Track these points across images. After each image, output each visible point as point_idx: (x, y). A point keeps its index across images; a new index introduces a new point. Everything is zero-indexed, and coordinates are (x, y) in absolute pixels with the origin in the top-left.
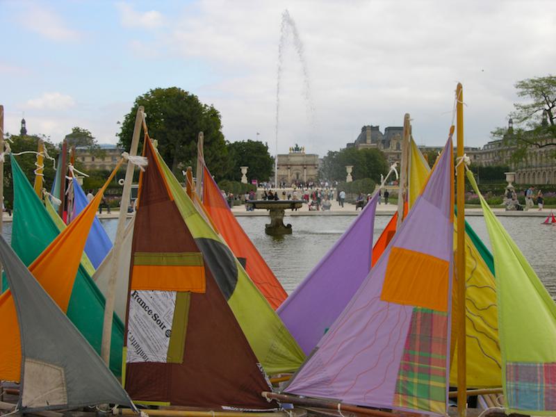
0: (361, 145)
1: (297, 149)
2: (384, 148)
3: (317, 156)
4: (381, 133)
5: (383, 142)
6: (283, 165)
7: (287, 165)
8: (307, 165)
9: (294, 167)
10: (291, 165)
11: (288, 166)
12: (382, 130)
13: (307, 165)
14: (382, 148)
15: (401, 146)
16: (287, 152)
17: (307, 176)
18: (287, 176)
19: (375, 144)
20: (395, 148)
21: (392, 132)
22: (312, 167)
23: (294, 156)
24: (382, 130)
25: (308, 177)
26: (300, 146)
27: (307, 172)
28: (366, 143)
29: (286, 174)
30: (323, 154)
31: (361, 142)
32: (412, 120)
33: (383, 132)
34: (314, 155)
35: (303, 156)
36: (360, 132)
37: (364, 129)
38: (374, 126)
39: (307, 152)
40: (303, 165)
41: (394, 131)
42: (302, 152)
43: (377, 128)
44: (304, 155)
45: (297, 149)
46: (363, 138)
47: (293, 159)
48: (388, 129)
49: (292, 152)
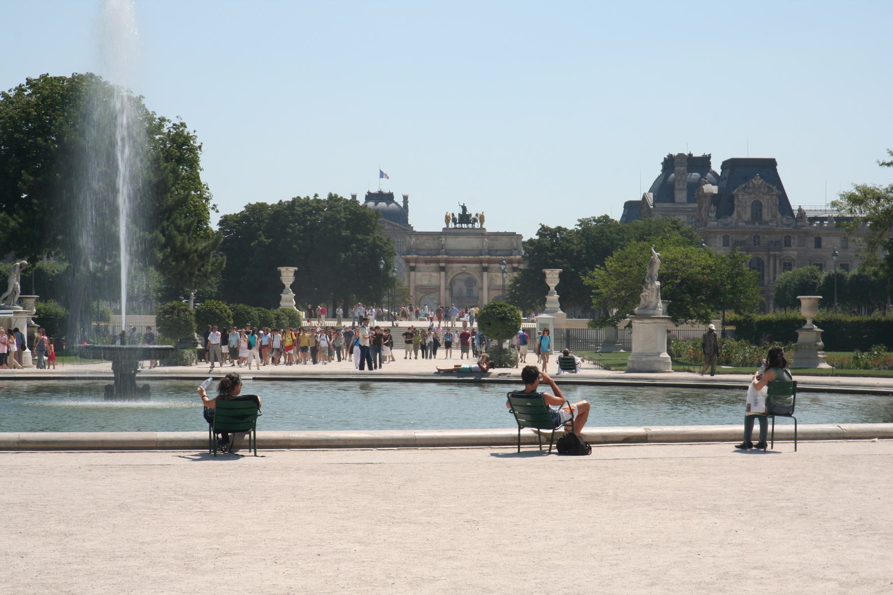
1: (465, 217)
2: (718, 217)
3: (520, 236)
4: (715, 174)
12: (716, 167)
13: (489, 262)
14: (713, 215)
15: (765, 211)
16: (438, 226)
19: (696, 205)
20: (747, 216)
24: (716, 167)
26: (472, 211)
28: (672, 200)
29: (434, 282)
30: (530, 233)
33: (719, 172)
37: (670, 163)
38: (697, 154)
39: (490, 226)
42: (477, 225)
44: (481, 233)
45: (465, 217)
46: (663, 189)
47: (453, 243)
48: (731, 165)
49: (451, 225)
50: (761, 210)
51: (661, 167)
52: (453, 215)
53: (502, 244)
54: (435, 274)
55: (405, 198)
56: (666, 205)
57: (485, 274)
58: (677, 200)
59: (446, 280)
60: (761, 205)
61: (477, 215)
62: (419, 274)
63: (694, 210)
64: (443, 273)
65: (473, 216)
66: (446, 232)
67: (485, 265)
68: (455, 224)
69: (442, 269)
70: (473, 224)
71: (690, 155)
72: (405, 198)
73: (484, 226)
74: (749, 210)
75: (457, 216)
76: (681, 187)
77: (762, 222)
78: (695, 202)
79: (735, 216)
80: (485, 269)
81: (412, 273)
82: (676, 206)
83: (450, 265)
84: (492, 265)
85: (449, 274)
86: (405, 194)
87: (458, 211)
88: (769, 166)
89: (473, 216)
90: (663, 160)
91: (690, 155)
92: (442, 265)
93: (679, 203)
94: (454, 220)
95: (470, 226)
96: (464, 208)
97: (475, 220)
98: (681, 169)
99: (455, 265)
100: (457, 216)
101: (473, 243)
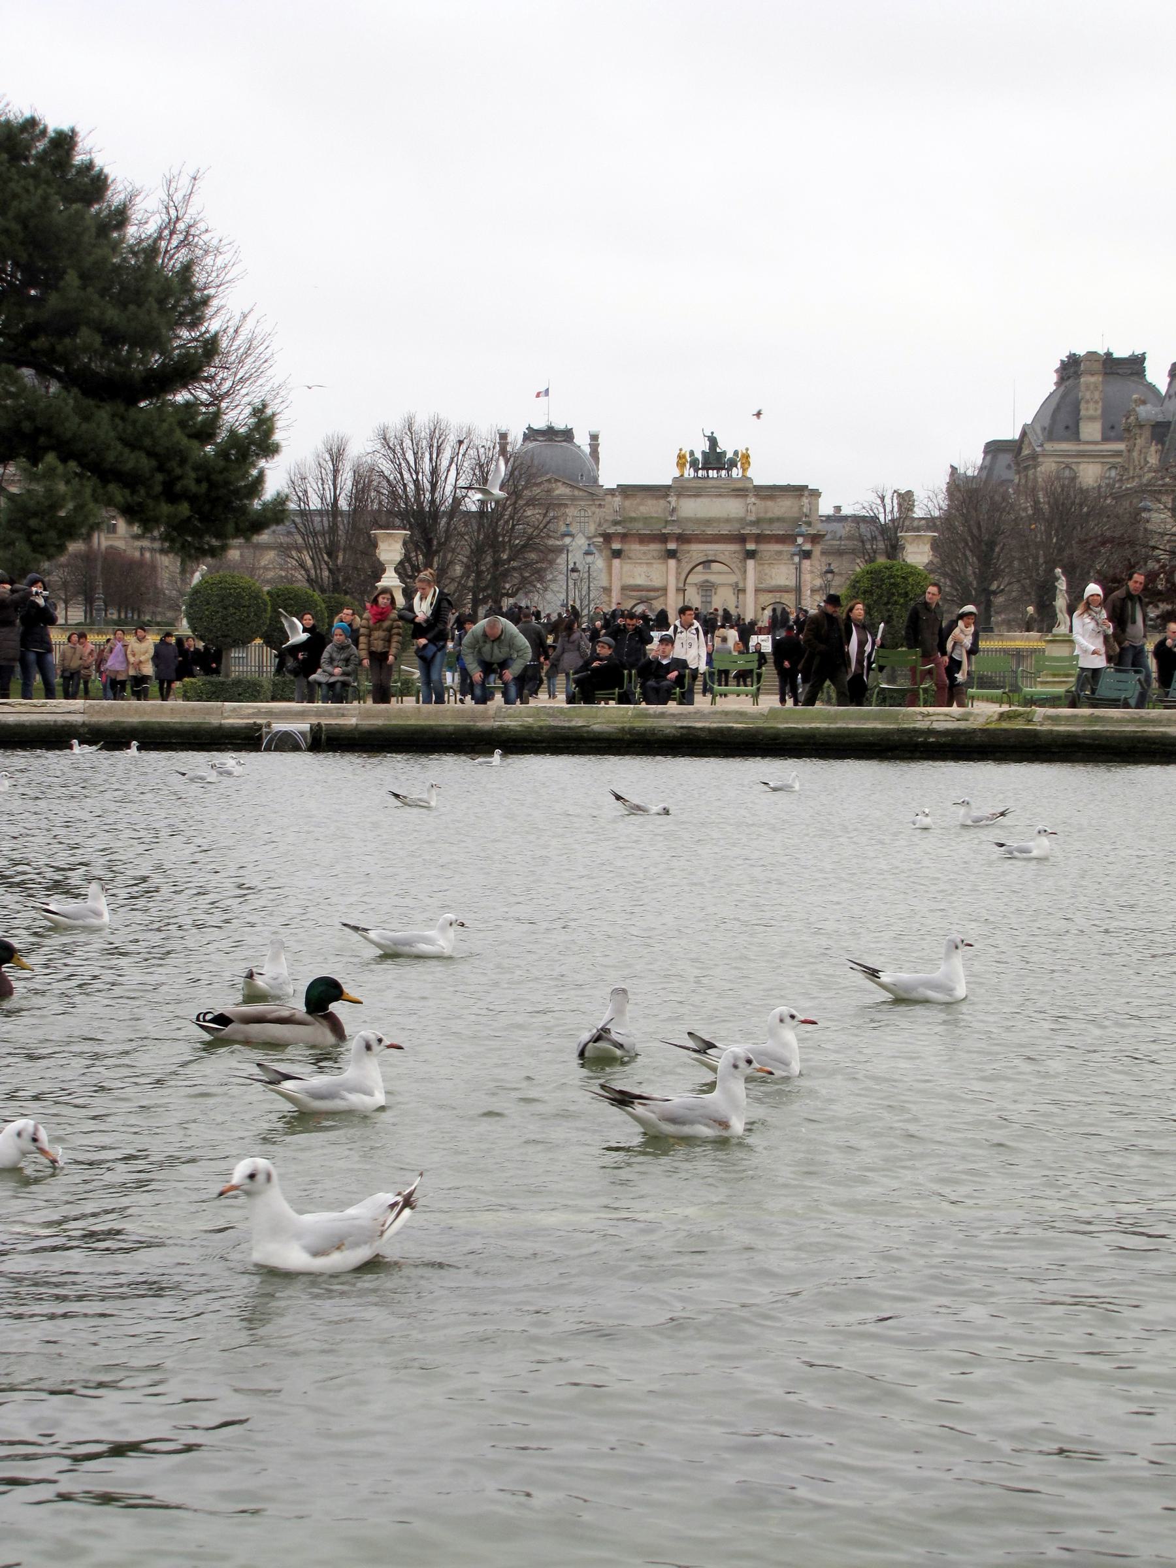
0: (1048, 446)
1: (714, 459)
4: (1152, 388)
6: (643, 539)
7: (663, 538)
8: (759, 538)
9: (698, 551)
10: (683, 539)
13: (759, 538)
16: (664, 473)
17: (757, 591)
18: (664, 590)
19: (1121, 446)
25: (767, 599)
26: (727, 446)
27: (760, 579)
28: (1075, 436)
34: (799, 491)
36: (1046, 384)
37: (1071, 368)
38: (1120, 353)
39: (761, 474)
40: (742, 539)
42: (736, 473)
43: (1136, 364)
44: (742, 490)
45: (714, 459)
46: (1061, 416)
47: (690, 508)
49: (689, 473)
51: (1054, 378)
52: (692, 453)
53: (783, 507)
55: (594, 437)
56: (1064, 446)
57: (751, 563)
59: (678, 573)
62: (627, 567)
63: (1118, 454)
64: (672, 563)
65: (730, 455)
66: (679, 489)
67: (751, 546)
68: (696, 471)
69: (672, 554)
70: (729, 470)
71: (1109, 355)
72: (594, 437)
73: (749, 474)
75: (699, 455)
76: (1091, 412)
78: (1120, 439)
80: (751, 555)
81: (616, 562)
83: (686, 547)
84: (763, 547)
85: (684, 564)
86: (594, 430)
87: (700, 447)
89: (730, 455)
90: (1058, 365)
92: (672, 546)
93: (1088, 443)
94: (694, 464)
95: (723, 473)
96: (713, 441)
97: (733, 463)
98: (1092, 379)
99: (694, 547)
100: (699, 455)
101: (732, 508)
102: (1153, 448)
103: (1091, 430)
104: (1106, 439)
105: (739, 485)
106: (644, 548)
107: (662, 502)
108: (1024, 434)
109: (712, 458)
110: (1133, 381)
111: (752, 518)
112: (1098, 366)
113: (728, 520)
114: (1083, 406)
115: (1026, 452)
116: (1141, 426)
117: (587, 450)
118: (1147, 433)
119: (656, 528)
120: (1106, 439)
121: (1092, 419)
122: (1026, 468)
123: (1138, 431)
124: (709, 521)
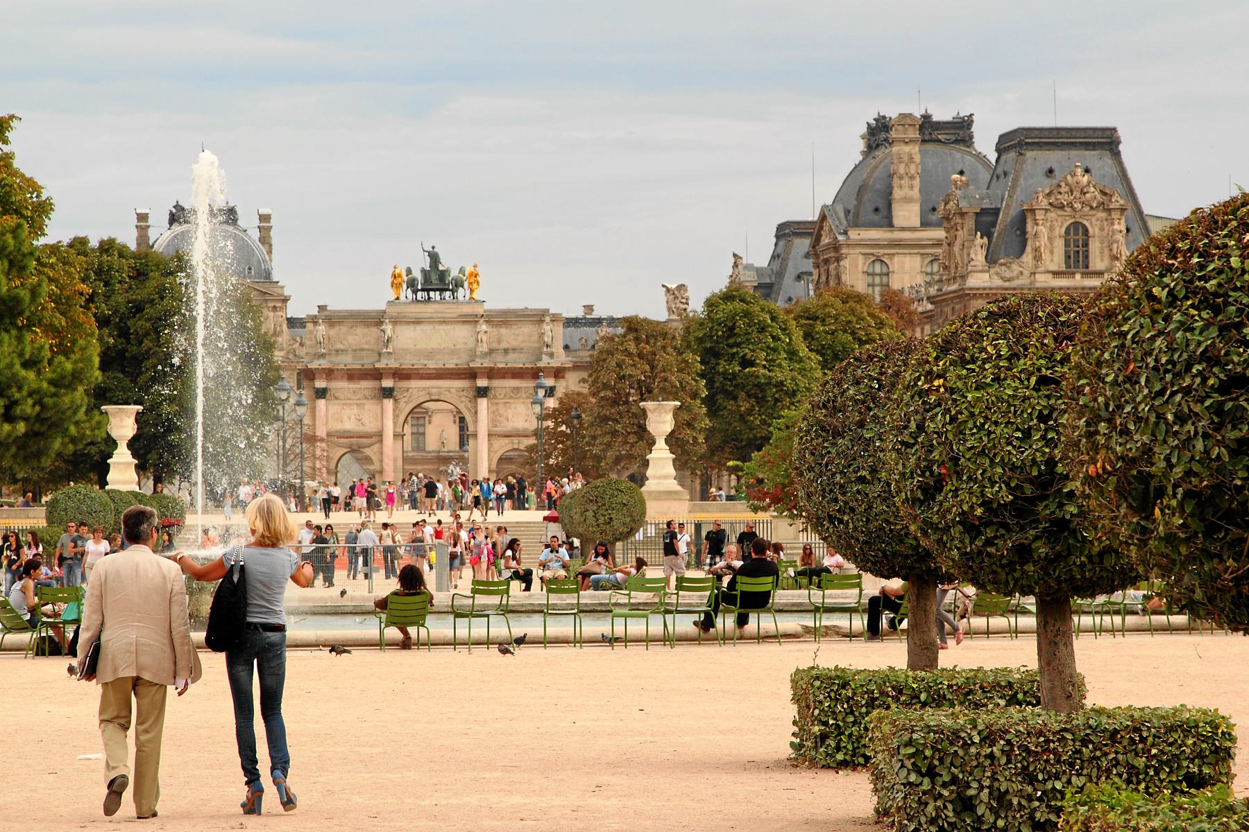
0: (854, 234)
1: (437, 280)
2: (991, 260)
4: (981, 158)
5: (986, 220)
6: (353, 375)
7: (377, 375)
9: (417, 389)
10: (401, 375)
11: (383, 380)
13: (492, 373)
14: (979, 257)
15: (1094, 246)
18: (379, 436)
19: (940, 234)
20: (1055, 258)
21: (1037, 159)
22: (528, 384)
23: (417, 322)
25: (503, 446)
26: (451, 264)
27: (494, 421)
31: (855, 219)
32: (676, 294)
35: (472, 320)
36: (850, 150)
38: (942, 114)
39: (495, 294)
40: (472, 374)
41: (1053, 158)
43: (960, 131)
45: (437, 280)
48: (1016, 142)
49: (406, 294)
50: (1086, 245)
51: (861, 145)
52: (409, 271)
54: (371, 406)
57: (483, 403)
58: (897, 222)
59: (396, 416)
60: (1086, 231)
61: (462, 271)
62: (334, 408)
63: (938, 244)
64: (389, 404)
65: (454, 273)
67: (482, 383)
68: (415, 292)
69: (388, 393)
70: (453, 291)
71: (926, 117)
74: (1059, 245)
75: (417, 274)
76: (906, 192)
77: (1088, 274)
78: (938, 225)
79: (1028, 258)
80: (482, 392)
81: (321, 403)
82: (897, 235)
83: (404, 384)
84: (496, 383)
85: (402, 404)
87: (420, 264)
88: (1105, 141)
89: (454, 273)
90: (864, 129)
91: (926, 117)
92: (387, 383)
93: (903, 229)
94: (412, 284)
95: (448, 294)
96: (434, 258)
97: (458, 284)
98: (906, 149)
99: (414, 384)
100: (417, 274)
102: (979, 241)
103: (907, 214)
104: (925, 224)
105: (467, 309)
106: (353, 386)
107: (374, 330)
108: (823, 218)
109: (434, 278)
110: (959, 151)
111: (484, 348)
112: (914, 134)
113: (453, 352)
114: (896, 182)
115: (825, 240)
116: (962, 214)
117: (255, 234)
118: (970, 223)
119: (368, 362)
120: (925, 224)
121: (907, 200)
122: (826, 261)
123: (959, 221)
124: (431, 354)
